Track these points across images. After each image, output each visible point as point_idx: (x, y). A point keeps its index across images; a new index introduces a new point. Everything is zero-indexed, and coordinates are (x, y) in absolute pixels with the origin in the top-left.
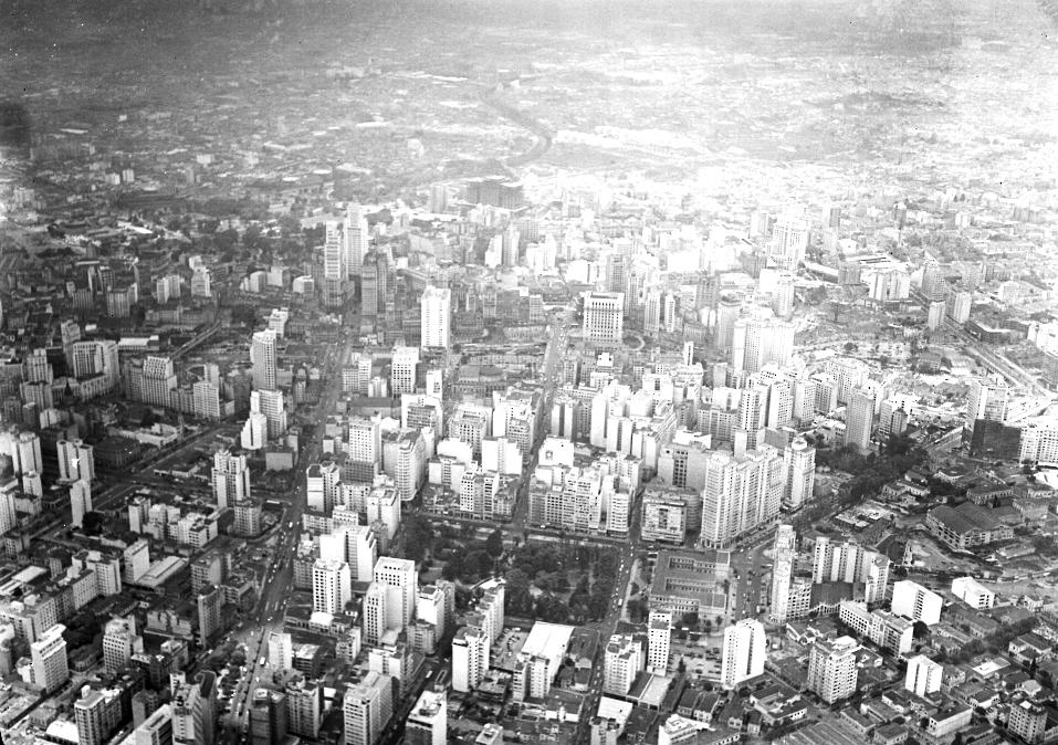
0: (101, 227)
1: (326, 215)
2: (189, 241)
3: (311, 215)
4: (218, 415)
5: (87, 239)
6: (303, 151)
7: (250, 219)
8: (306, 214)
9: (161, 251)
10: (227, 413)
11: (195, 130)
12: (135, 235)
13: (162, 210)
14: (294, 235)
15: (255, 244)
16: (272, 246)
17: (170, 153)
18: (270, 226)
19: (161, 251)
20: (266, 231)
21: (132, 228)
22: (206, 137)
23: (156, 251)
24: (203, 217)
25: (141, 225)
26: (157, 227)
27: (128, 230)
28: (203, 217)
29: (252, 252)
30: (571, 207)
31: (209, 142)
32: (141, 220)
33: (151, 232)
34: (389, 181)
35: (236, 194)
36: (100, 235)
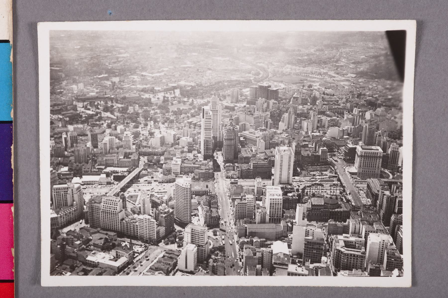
0: (69, 110)
1: (180, 105)
2: (116, 118)
3: (172, 104)
4: (155, 238)
5: (61, 117)
6: (160, 76)
7: (143, 106)
8: (170, 104)
9: (101, 122)
10: (161, 236)
11: (110, 68)
12: (87, 114)
13: (99, 102)
14: (167, 114)
15: (149, 119)
16: (158, 120)
17: (100, 77)
18: (154, 109)
19: (101, 122)
20: (152, 112)
21: (84, 111)
22: (116, 71)
23: (98, 123)
24: (120, 106)
25: (89, 109)
26: (97, 110)
27: (83, 112)
28: (120, 106)
29: (149, 123)
30: (302, 99)
31: (117, 73)
32: (89, 107)
33: (94, 113)
34: (204, 89)
35: (133, 95)
36: (68, 115)
